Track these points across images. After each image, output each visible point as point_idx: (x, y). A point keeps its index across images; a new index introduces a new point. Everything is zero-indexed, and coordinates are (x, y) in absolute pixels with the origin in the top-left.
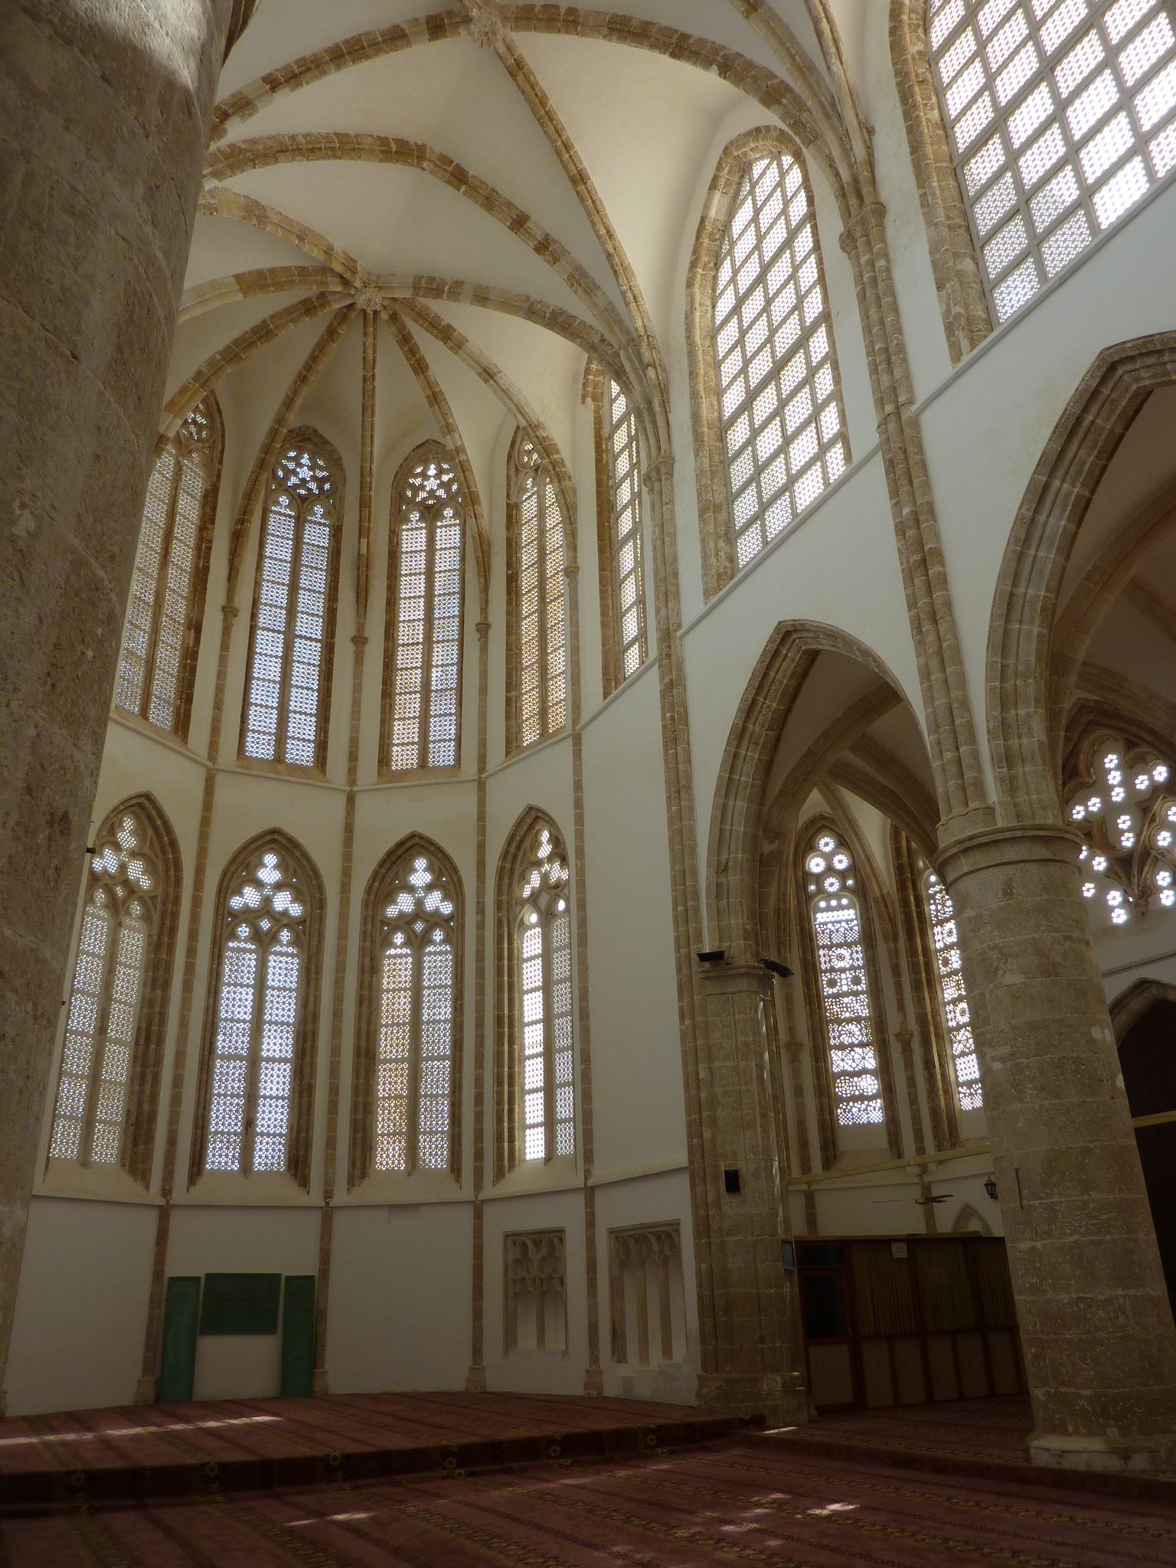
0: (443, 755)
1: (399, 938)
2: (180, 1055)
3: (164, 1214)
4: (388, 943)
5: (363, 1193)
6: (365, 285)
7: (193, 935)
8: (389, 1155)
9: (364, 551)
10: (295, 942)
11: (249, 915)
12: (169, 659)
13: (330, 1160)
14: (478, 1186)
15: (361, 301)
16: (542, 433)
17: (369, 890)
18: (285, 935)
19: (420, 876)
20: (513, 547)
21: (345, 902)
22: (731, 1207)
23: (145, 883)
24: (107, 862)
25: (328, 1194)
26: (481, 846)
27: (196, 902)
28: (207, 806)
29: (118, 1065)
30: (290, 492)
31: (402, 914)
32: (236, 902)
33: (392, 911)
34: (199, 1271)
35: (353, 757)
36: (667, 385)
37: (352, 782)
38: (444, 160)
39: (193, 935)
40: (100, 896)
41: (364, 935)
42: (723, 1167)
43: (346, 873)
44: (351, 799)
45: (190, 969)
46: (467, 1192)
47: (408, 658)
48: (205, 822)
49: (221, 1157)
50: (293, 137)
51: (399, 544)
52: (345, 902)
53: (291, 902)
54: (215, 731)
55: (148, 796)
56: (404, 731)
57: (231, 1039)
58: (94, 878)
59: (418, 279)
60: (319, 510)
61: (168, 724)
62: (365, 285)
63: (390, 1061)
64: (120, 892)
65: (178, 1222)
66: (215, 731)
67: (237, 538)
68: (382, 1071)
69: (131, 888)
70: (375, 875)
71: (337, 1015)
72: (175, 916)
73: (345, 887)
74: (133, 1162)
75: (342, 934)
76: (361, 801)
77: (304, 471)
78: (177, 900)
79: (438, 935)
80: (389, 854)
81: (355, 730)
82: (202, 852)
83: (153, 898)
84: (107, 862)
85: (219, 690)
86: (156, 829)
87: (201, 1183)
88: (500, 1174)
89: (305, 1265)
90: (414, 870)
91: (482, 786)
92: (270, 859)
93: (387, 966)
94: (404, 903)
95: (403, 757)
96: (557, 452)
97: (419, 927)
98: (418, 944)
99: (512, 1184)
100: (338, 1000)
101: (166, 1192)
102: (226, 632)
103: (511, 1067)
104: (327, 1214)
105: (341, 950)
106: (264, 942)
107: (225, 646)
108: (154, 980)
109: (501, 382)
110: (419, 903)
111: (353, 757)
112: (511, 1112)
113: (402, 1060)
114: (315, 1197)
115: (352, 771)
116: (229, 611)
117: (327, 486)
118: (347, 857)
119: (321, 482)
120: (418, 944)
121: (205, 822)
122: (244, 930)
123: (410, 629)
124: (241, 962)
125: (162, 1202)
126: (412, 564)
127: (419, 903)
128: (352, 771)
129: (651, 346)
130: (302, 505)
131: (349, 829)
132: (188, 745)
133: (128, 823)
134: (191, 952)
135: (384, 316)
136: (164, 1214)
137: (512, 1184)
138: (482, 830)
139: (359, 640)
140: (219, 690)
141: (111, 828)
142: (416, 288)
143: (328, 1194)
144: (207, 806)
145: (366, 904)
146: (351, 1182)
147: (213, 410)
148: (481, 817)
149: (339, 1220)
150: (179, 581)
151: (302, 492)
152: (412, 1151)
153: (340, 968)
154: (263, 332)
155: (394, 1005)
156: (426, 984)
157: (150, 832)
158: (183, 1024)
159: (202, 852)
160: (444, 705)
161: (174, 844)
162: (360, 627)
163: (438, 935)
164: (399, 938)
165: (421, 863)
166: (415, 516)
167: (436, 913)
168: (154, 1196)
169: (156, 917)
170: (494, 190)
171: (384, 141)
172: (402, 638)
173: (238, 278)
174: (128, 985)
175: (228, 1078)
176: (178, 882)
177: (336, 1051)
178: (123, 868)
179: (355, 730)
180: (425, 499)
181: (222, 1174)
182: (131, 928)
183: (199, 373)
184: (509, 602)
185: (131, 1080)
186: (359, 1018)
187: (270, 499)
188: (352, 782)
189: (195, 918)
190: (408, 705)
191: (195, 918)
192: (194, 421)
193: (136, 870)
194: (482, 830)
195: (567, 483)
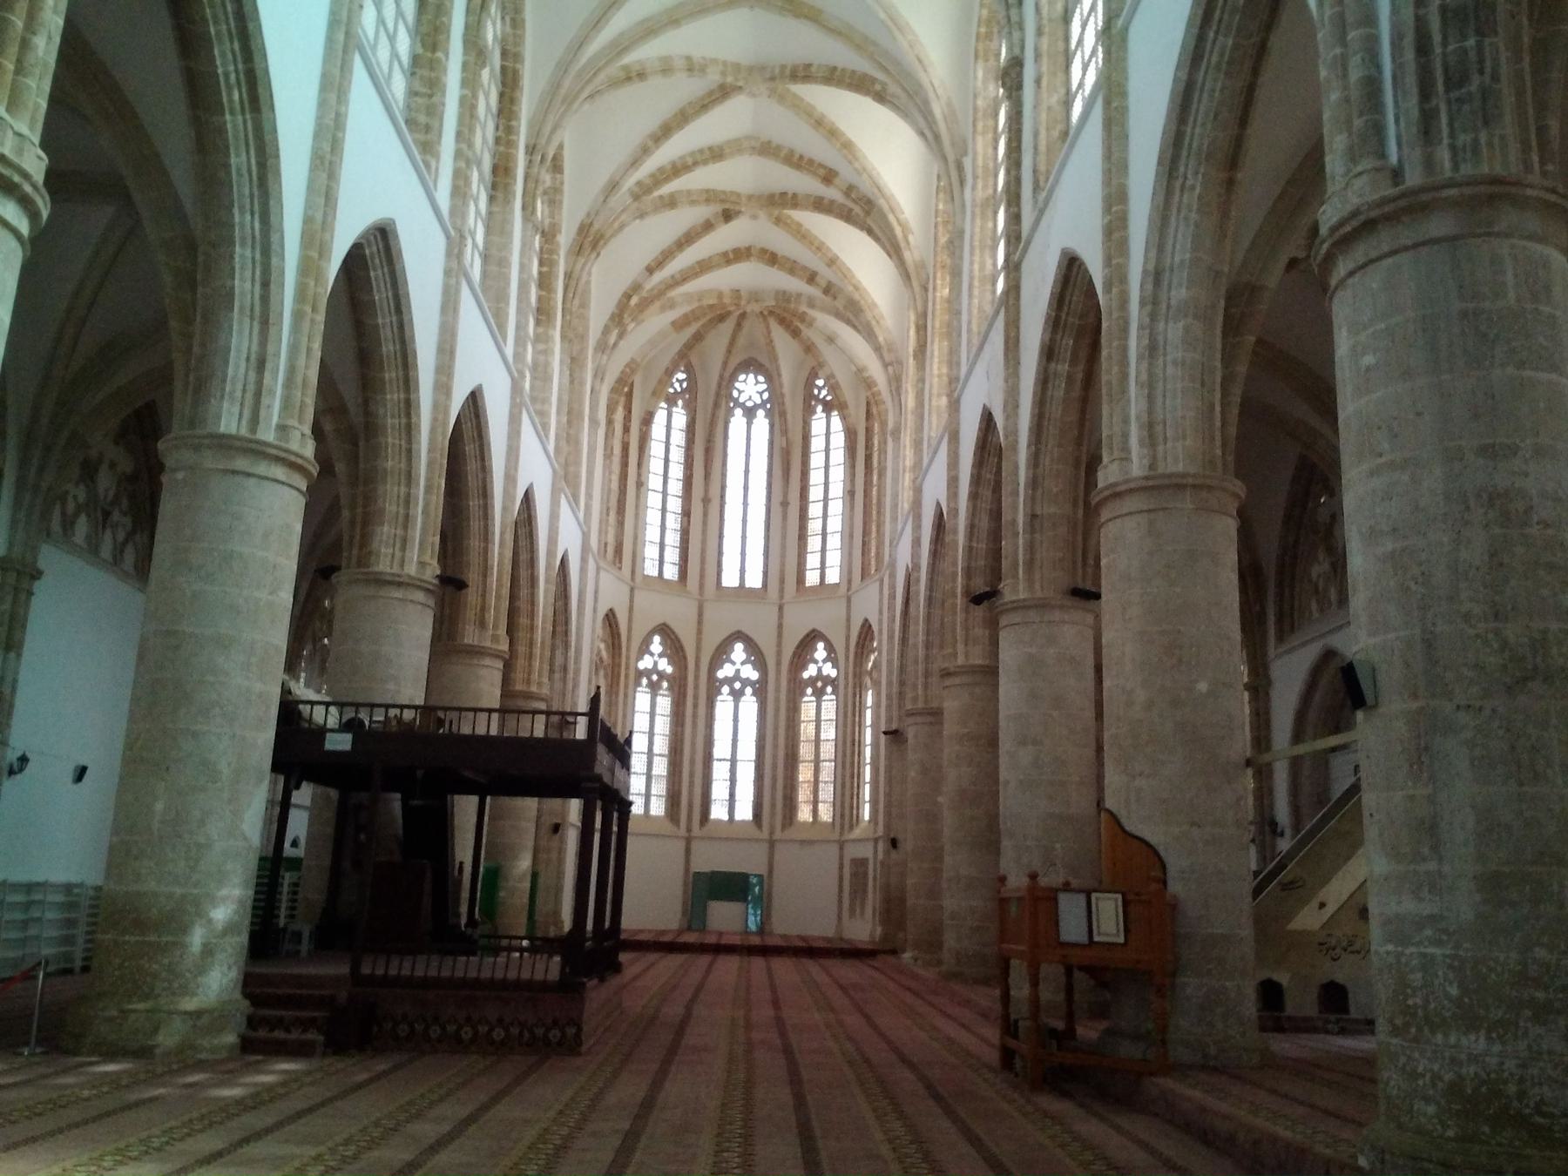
0: (833, 577)
1: (809, 691)
2: (692, 762)
3: (688, 841)
4: (803, 694)
5: (791, 833)
6: (749, 302)
7: (696, 697)
8: (804, 814)
9: (784, 445)
10: (754, 694)
11: (729, 681)
12: (673, 538)
13: (773, 814)
14: (841, 834)
15: (748, 310)
16: (866, 374)
17: (792, 663)
18: (749, 690)
19: (820, 652)
20: (869, 431)
21: (778, 672)
22: (894, 855)
23: (669, 670)
24: (646, 663)
25: (772, 833)
26: (848, 638)
27: (697, 677)
28: (700, 622)
29: (661, 767)
30: (743, 406)
31: (811, 677)
32: (721, 674)
33: (806, 675)
34: (706, 869)
35: (782, 581)
36: (900, 376)
37: (782, 597)
38: (764, 251)
39: (696, 697)
40: (645, 681)
41: (789, 691)
42: (892, 836)
43: (779, 653)
44: (781, 608)
45: (695, 716)
46: (836, 836)
47: (815, 510)
48: (699, 632)
49: (718, 812)
50: (673, 277)
51: (810, 431)
52: (778, 672)
53: (721, 694)
54: (702, 576)
55: (664, 624)
56: (813, 561)
57: (721, 749)
58: (640, 674)
59: (777, 293)
60: (761, 413)
61: (676, 578)
62: (749, 302)
63: (806, 761)
64: (655, 677)
65: (695, 845)
66: (702, 576)
67: (708, 451)
68: (801, 767)
69: (662, 675)
70: (795, 654)
71: (776, 737)
72: (685, 685)
73: (779, 663)
74: (671, 815)
75: (777, 690)
76: (786, 608)
77: (750, 388)
78: (685, 678)
79: (829, 689)
80: (802, 642)
81: (783, 565)
82: (698, 649)
83: (674, 678)
84: (646, 663)
85: (703, 551)
86: (671, 639)
87: (705, 829)
88: (851, 828)
89: (763, 871)
90: (816, 650)
91: (849, 600)
92: (739, 647)
93: (804, 707)
94: (810, 671)
95: (812, 578)
96: (876, 386)
97: (819, 684)
98: (819, 694)
99: (857, 833)
100: (776, 728)
101: (689, 830)
102: (705, 514)
103: (859, 768)
104: (772, 844)
105: (777, 700)
106: (737, 695)
107: (705, 523)
108: (677, 720)
109: (839, 344)
110: (820, 670)
111: (782, 581)
112: (858, 794)
113: (811, 761)
114: (765, 834)
115: (782, 590)
116: (706, 501)
117: (766, 396)
118: (779, 644)
119: (761, 394)
120: (819, 694)
121: (699, 632)
122: (726, 689)
123: (815, 493)
124: (723, 706)
125: (687, 835)
126: (817, 444)
127: (820, 670)
128: (782, 590)
129: (890, 350)
130: (750, 413)
131: (780, 626)
132: (688, 588)
133: (657, 639)
134: (695, 706)
135: (766, 313)
136: (688, 841)
137: (857, 833)
138: (848, 628)
139: (785, 504)
140: (703, 551)
141: (647, 642)
142: (776, 299)
143: (772, 833)
144: (700, 622)
145: (790, 671)
146: (784, 827)
147: (689, 370)
148: (848, 620)
149: (778, 846)
150: (676, 487)
151: (749, 404)
152: (815, 812)
153: (777, 710)
154: (698, 337)
155: (807, 730)
156: (823, 718)
157: (669, 642)
158: (693, 744)
159: (698, 649)
160: (834, 542)
161: (682, 648)
162: (785, 494)
163: (829, 689)
164: (809, 691)
165: (821, 645)
166: (820, 408)
167: (828, 676)
168: (683, 831)
169: (676, 689)
170: (795, 262)
171: (725, 254)
172: (812, 498)
173: (673, 323)
174: (663, 725)
175: (720, 771)
176: (686, 668)
177: (775, 757)
178: (656, 663)
179: (783, 565)
180: (825, 397)
181: (719, 822)
182: (663, 695)
183: (667, 369)
184: (866, 474)
185: (669, 772)
186: (787, 738)
187: (730, 412)
188: (782, 597)
189: (696, 687)
190: (814, 543)
191: (696, 687)
192: (677, 380)
193: (665, 666)
194: (848, 628)
195: (882, 407)
